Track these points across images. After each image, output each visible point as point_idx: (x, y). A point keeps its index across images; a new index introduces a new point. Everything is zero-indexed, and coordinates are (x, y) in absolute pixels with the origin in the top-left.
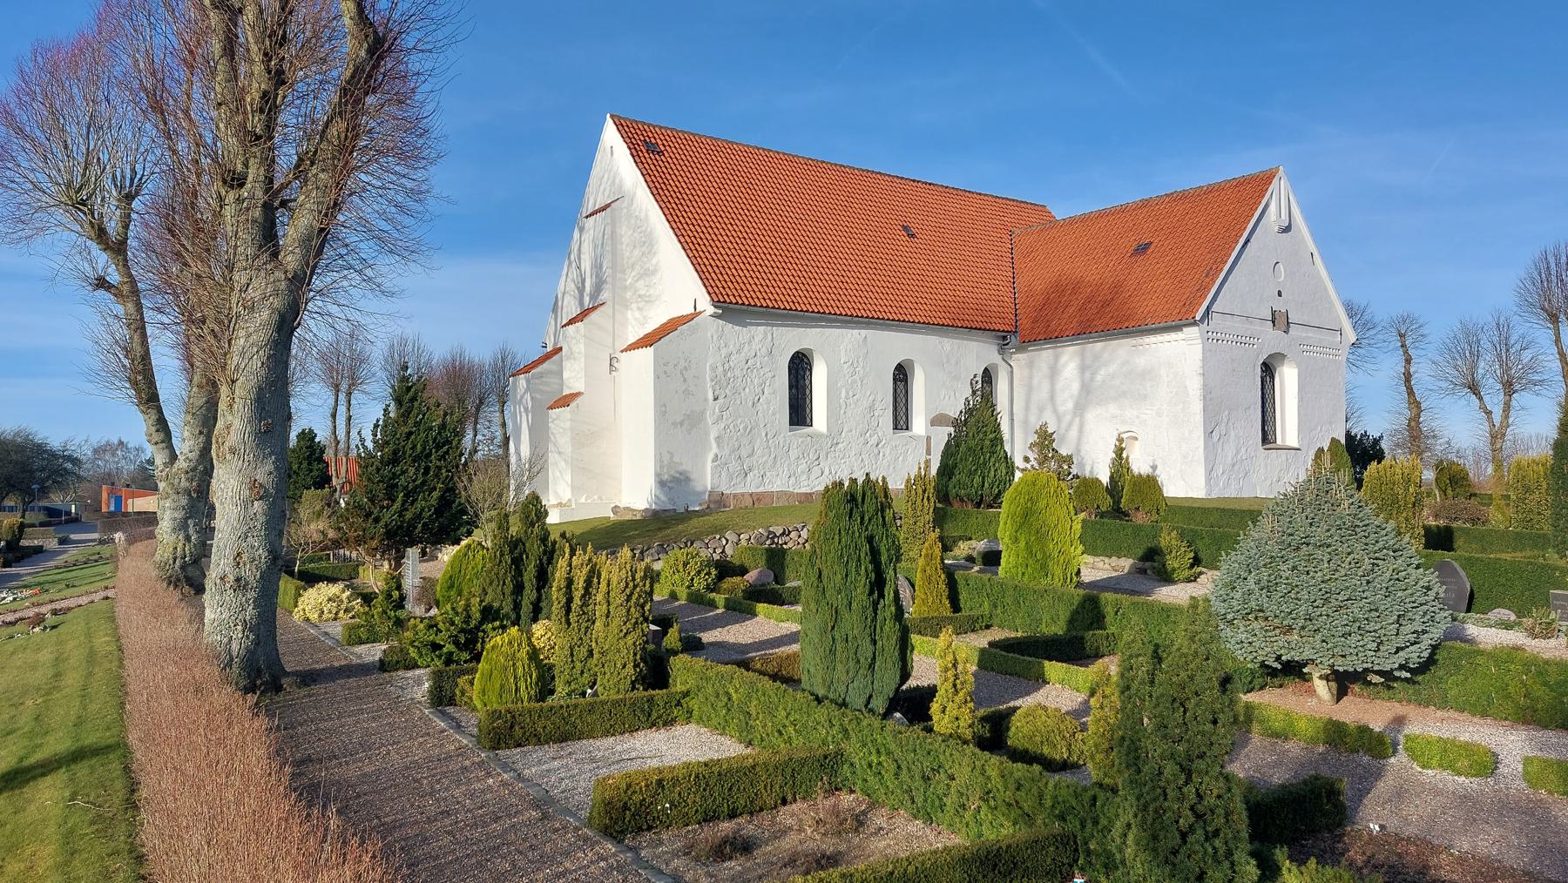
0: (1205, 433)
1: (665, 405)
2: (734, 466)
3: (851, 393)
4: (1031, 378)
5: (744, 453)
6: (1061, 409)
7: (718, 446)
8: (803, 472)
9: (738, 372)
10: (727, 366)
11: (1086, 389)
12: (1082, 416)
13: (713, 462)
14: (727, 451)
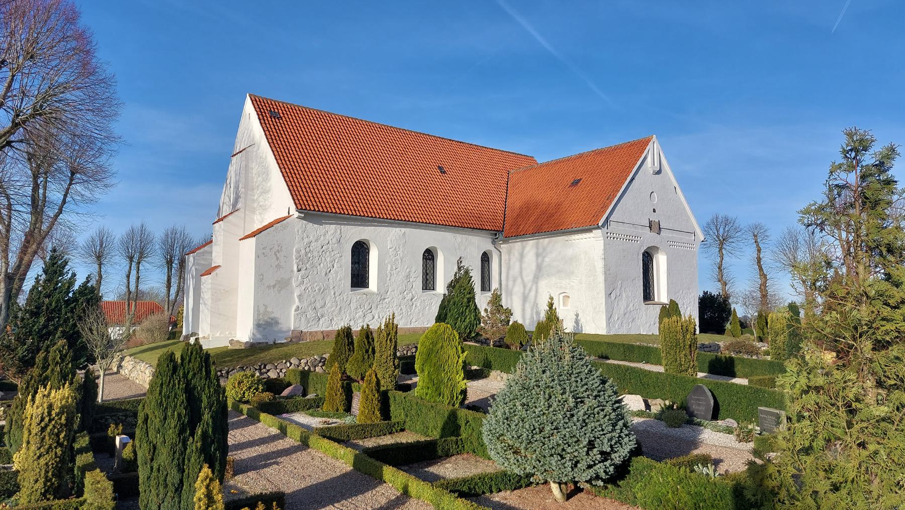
0: (606, 294)
1: (262, 275)
2: (311, 314)
3: (394, 268)
4: (510, 260)
5: (318, 305)
6: (526, 279)
7: (300, 300)
8: (360, 317)
9: (315, 254)
10: (308, 250)
11: (539, 268)
12: (537, 283)
13: (295, 311)
14: (305, 304)
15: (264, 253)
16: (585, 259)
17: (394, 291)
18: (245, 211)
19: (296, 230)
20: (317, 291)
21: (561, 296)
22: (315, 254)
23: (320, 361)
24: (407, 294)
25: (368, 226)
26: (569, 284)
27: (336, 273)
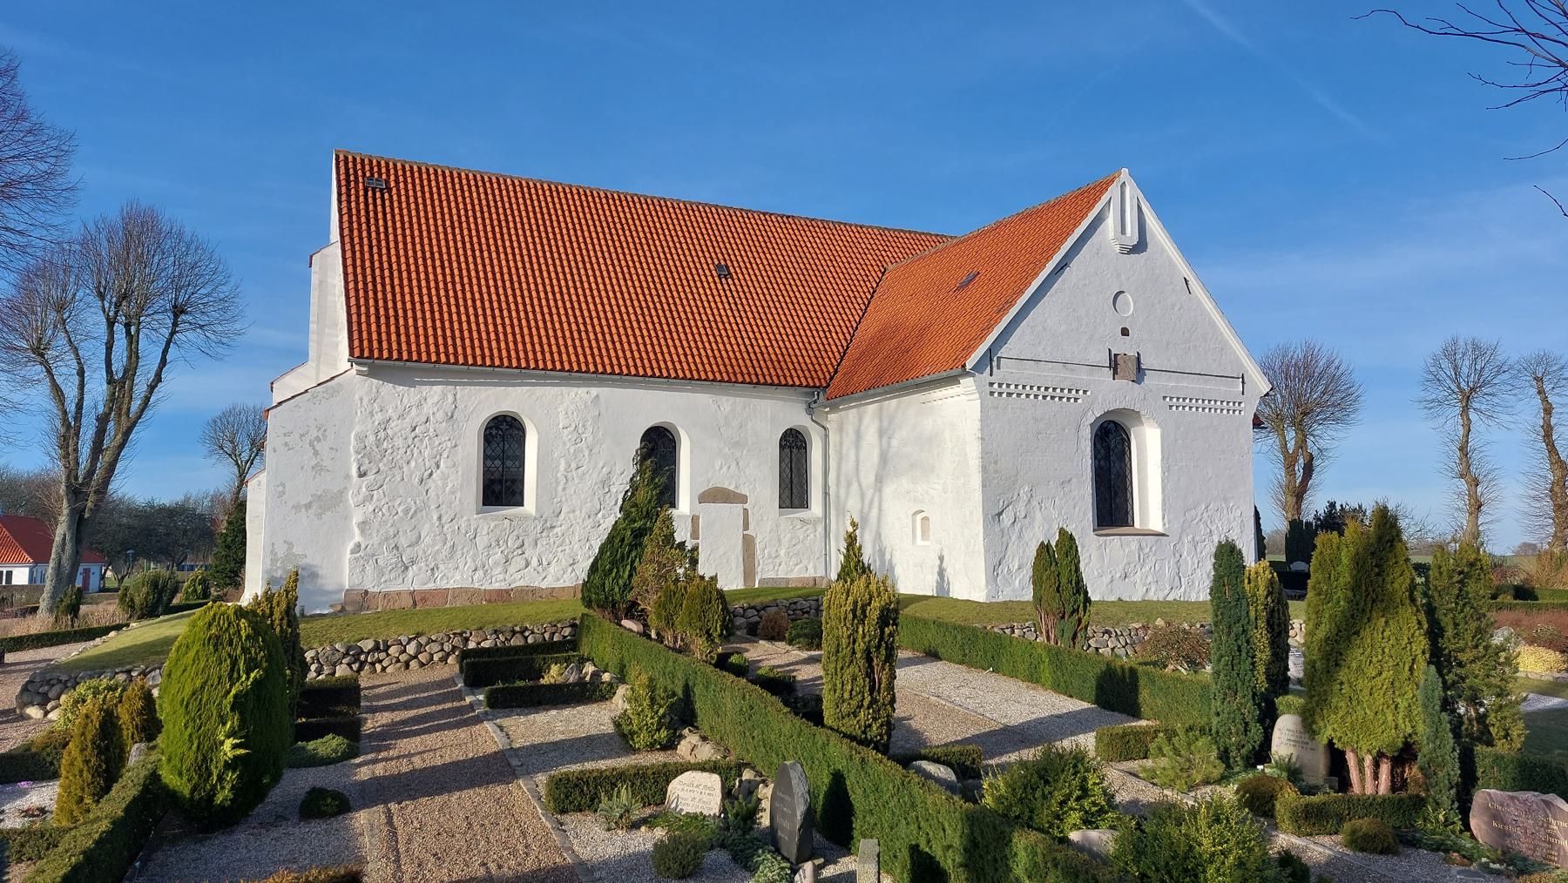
0: (985, 515)
1: (283, 485)
2: (386, 557)
3: (574, 466)
5: (403, 541)
7: (363, 532)
8: (496, 564)
9: (399, 442)
10: (382, 435)
13: (352, 552)
14: (375, 540)
15: (286, 444)
16: (951, 441)
17: (574, 511)
18: (318, 365)
19: (357, 397)
20: (400, 514)
21: (919, 517)
22: (399, 442)
23: (346, 654)
24: (603, 516)
25: (514, 385)
26: (927, 493)
27: (445, 478)
